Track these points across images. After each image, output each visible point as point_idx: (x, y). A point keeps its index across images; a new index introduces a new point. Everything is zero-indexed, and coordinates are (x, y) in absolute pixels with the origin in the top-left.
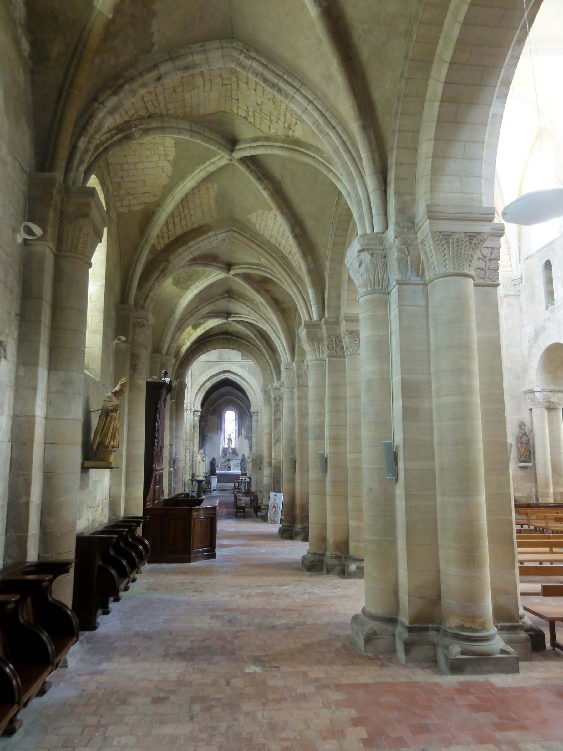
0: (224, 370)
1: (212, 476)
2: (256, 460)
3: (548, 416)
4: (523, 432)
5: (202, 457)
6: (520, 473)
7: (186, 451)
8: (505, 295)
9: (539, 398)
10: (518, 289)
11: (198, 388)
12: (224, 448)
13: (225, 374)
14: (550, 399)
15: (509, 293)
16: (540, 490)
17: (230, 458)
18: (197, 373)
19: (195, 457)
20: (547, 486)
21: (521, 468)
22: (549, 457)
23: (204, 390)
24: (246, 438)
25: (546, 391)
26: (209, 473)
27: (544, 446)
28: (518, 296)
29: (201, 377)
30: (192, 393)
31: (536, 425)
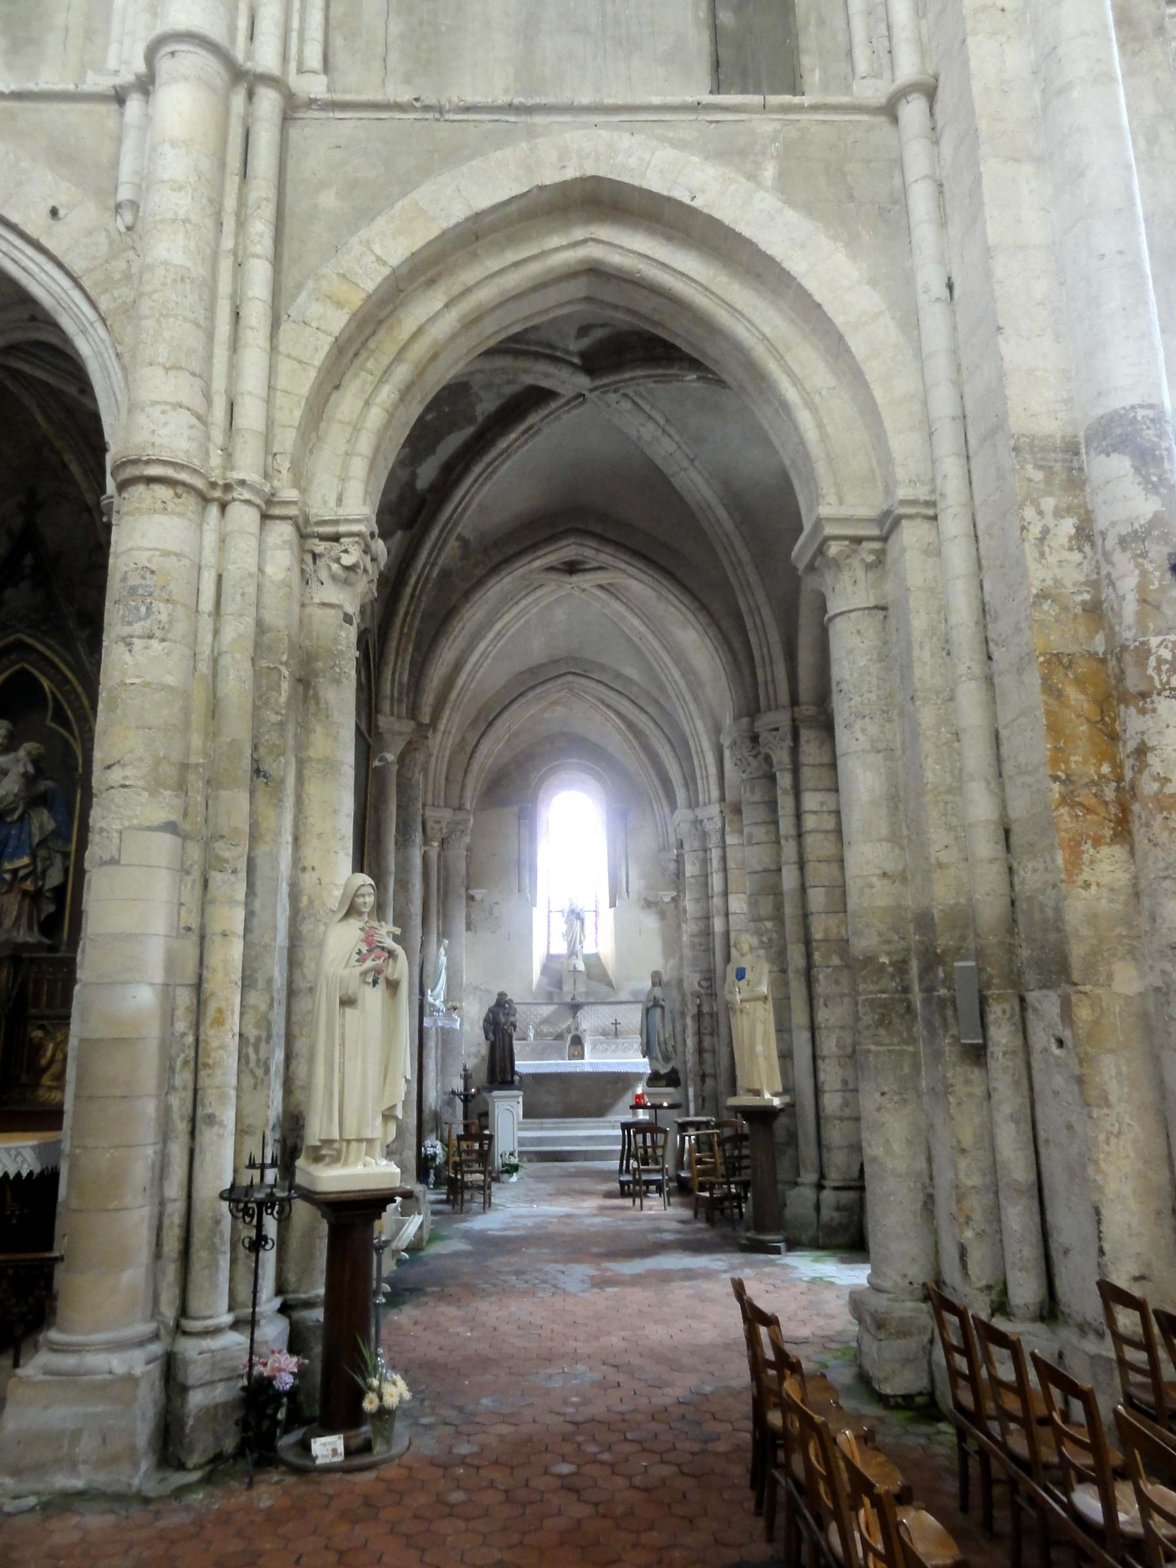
0: (570, 173)
1: (496, 1093)
2: (901, 967)
5: (372, 945)
7: (206, 884)
11: (338, 321)
12: (550, 958)
13: (579, 233)
17: (580, 999)
18: (328, 200)
19: (307, 953)
23: (399, 357)
24: (648, 904)
26: (482, 1076)
29: (363, 234)
30: (285, 367)
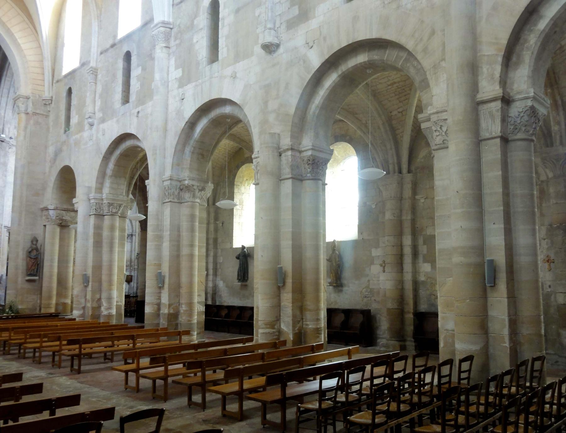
3: (61, 232)
4: (34, 246)
6: (27, 286)
8: (34, 112)
9: (52, 216)
10: (49, 109)
14: (62, 217)
15: (38, 112)
16: (43, 302)
20: (50, 298)
21: (29, 281)
22: (56, 270)
25: (58, 210)
27: (52, 261)
28: (47, 116)
31: (47, 241)
